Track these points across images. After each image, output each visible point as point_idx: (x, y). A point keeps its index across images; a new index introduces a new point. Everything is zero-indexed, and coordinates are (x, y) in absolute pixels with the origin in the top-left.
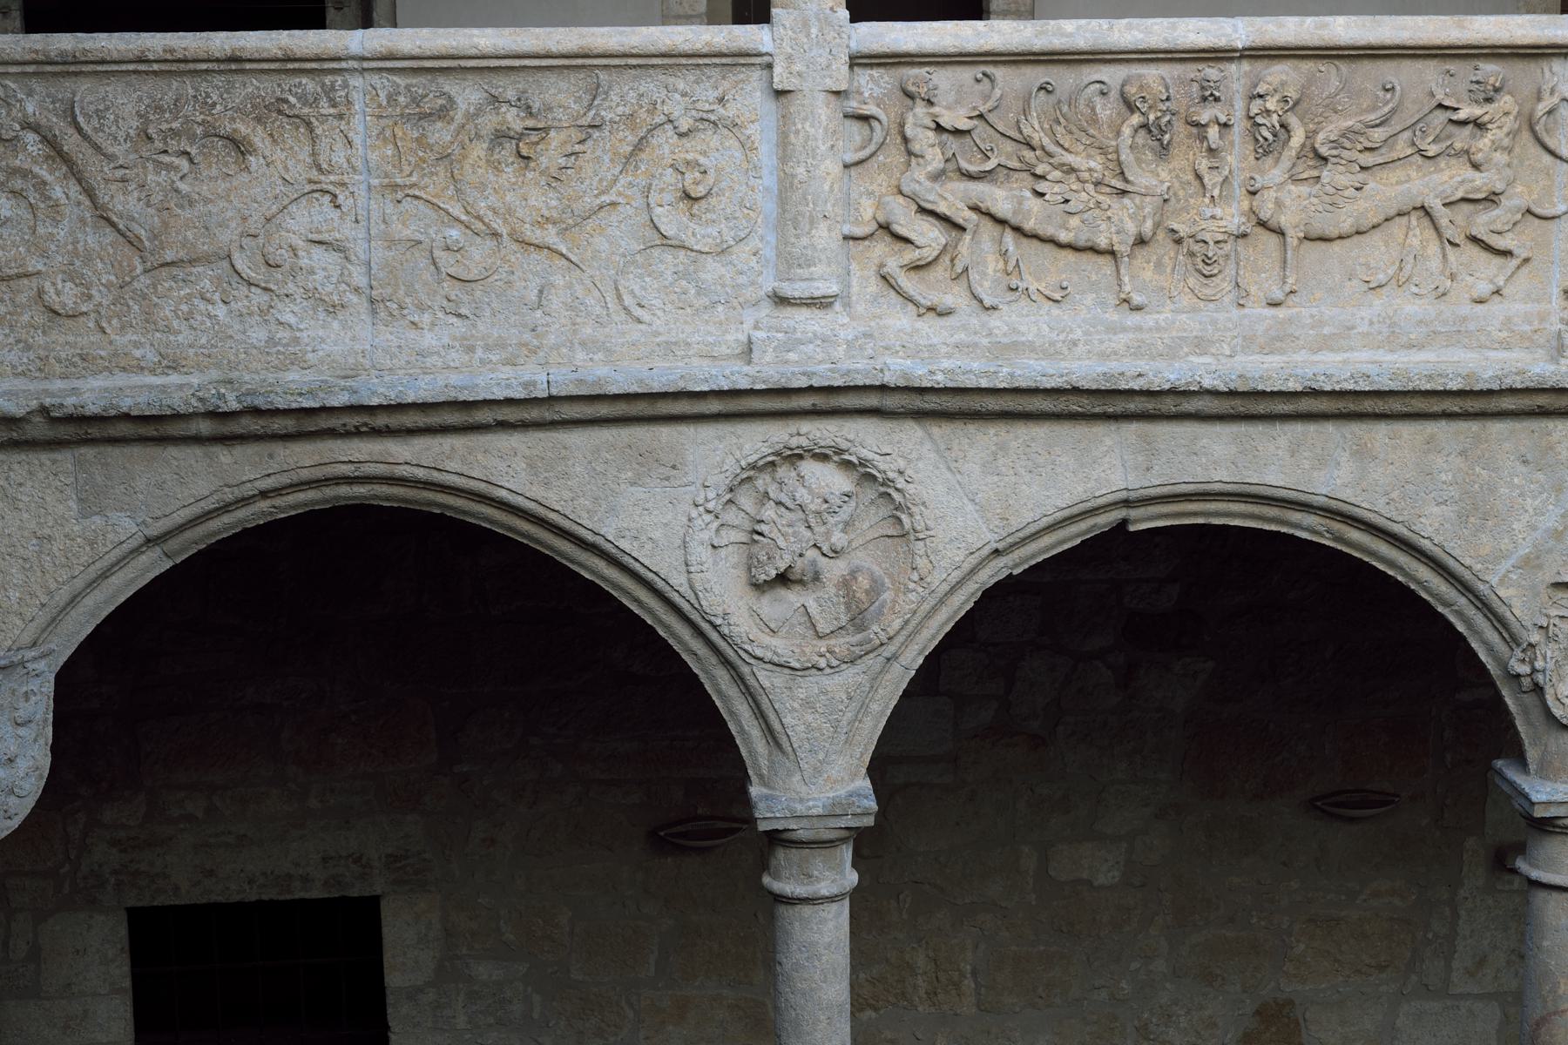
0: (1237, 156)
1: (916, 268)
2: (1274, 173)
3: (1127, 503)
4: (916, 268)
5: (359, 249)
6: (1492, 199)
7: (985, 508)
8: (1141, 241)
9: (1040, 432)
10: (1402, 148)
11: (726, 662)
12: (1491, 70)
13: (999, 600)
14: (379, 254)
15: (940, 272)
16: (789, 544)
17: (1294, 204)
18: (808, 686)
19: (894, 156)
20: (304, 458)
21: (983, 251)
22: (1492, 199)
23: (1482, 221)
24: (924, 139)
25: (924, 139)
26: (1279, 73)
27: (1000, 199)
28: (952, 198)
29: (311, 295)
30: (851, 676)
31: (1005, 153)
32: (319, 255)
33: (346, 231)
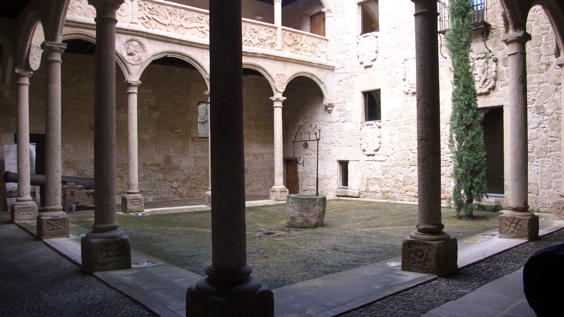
0: (179, 18)
1: (146, 23)
2: (182, 20)
3: (168, 52)
4: (146, 23)
5: (83, 8)
6: (203, 28)
7: (154, 50)
8: (169, 25)
9: (159, 42)
10: (194, 21)
11: (124, 64)
12: (203, 15)
13: (154, 62)
14: (86, 9)
15: (148, 24)
16: (132, 49)
17: (184, 24)
18: (134, 67)
19: (143, 10)
20: (76, 30)
21: (152, 22)
22: (203, 28)
23: (202, 30)
24: (147, 9)
25: (147, 9)
26: (182, 10)
27: (156, 17)
28: (150, 16)
29: (77, 13)
30: (138, 66)
31: (155, 13)
32: (78, 8)
33: (81, 6)
